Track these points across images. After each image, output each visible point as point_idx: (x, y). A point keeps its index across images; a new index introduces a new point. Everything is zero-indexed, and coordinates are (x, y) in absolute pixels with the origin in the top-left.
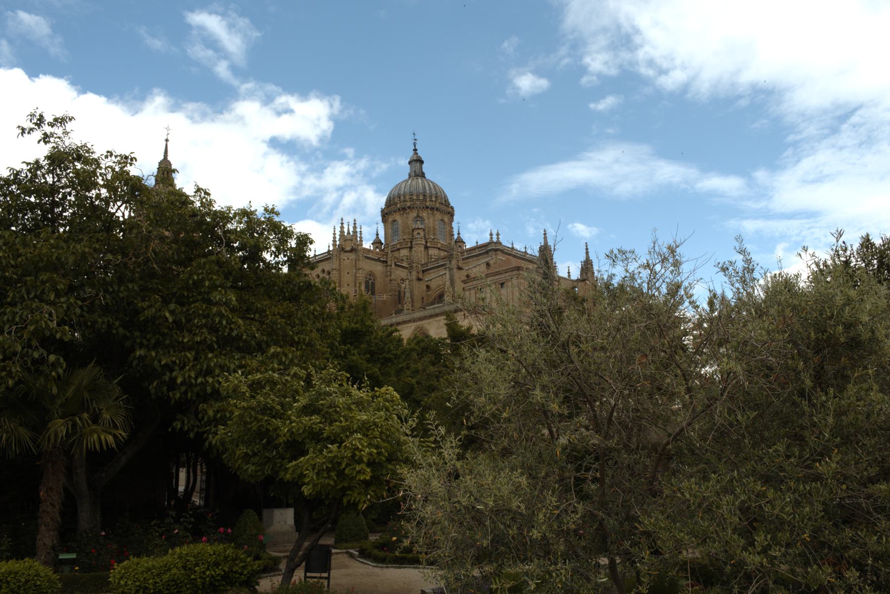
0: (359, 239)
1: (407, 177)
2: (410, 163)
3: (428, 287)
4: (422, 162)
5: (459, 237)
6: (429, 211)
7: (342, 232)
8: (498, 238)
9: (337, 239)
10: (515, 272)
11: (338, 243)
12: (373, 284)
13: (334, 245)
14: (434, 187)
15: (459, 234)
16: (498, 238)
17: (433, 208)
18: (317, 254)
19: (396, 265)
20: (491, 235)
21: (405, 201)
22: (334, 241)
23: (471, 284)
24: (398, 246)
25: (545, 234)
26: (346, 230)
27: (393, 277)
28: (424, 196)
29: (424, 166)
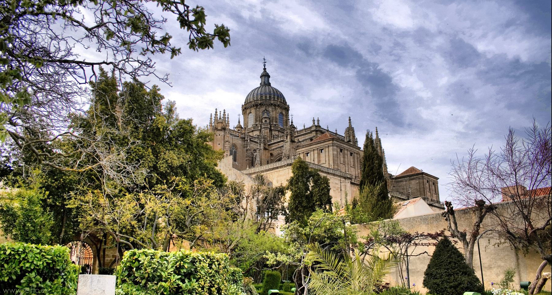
1: (259, 86)
2: (261, 77)
3: (271, 154)
4: (269, 77)
6: (273, 107)
8: (318, 123)
10: (331, 142)
15: (292, 122)
16: (318, 123)
17: (276, 105)
20: (314, 121)
21: (257, 100)
23: (301, 150)
24: (252, 129)
25: (350, 120)
26: (218, 116)
29: (270, 79)
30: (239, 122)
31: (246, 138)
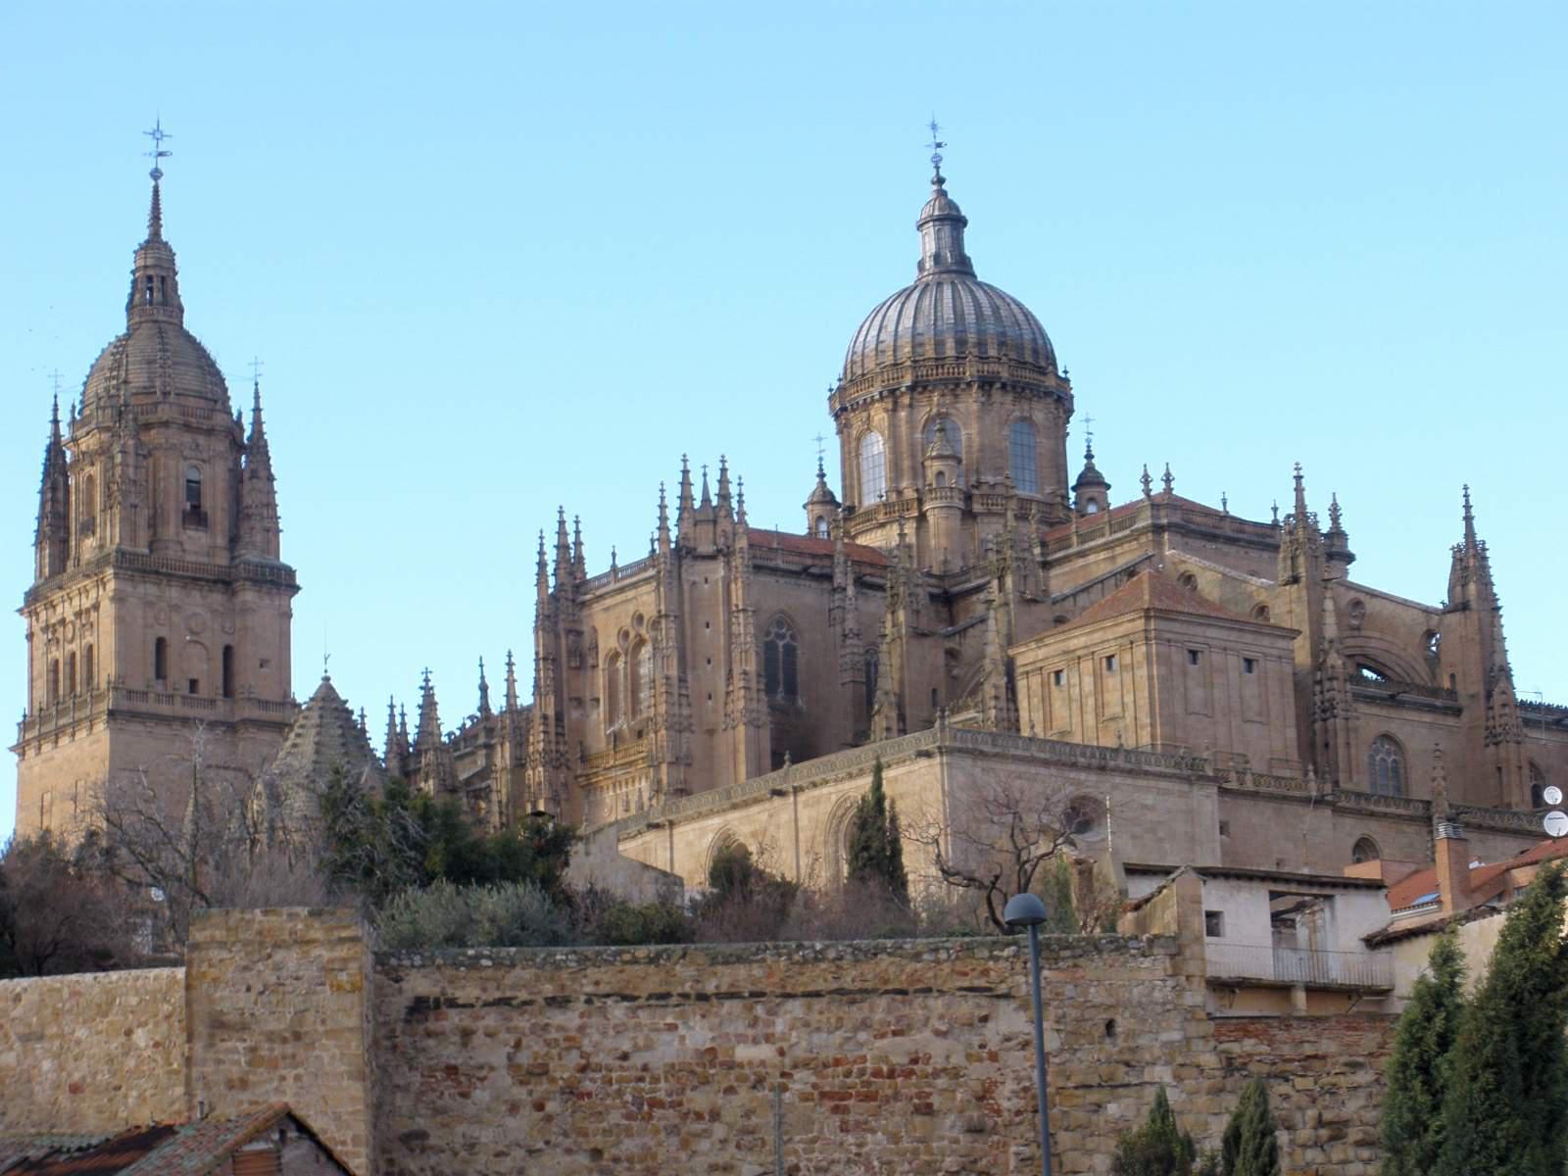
0: (736, 518)
5: (1089, 468)
7: (685, 497)
9: (672, 523)
11: (674, 534)
12: (790, 651)
13: (664, 540)
14: (996, 310)
15: (1089, 456)
18: (620, 564)
19: (860, 583)
22: (663, 528)
26: (697, 493)
27: (850, 624)
28: (961, 343)
30: (822, 475)
31: (838, 579)
